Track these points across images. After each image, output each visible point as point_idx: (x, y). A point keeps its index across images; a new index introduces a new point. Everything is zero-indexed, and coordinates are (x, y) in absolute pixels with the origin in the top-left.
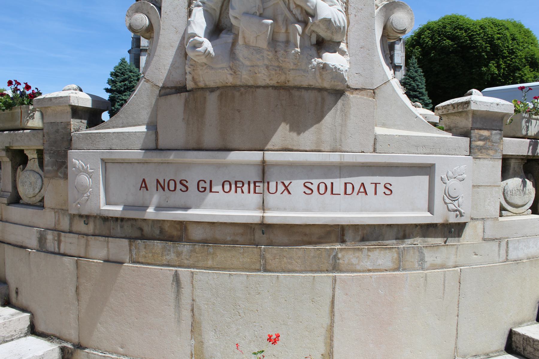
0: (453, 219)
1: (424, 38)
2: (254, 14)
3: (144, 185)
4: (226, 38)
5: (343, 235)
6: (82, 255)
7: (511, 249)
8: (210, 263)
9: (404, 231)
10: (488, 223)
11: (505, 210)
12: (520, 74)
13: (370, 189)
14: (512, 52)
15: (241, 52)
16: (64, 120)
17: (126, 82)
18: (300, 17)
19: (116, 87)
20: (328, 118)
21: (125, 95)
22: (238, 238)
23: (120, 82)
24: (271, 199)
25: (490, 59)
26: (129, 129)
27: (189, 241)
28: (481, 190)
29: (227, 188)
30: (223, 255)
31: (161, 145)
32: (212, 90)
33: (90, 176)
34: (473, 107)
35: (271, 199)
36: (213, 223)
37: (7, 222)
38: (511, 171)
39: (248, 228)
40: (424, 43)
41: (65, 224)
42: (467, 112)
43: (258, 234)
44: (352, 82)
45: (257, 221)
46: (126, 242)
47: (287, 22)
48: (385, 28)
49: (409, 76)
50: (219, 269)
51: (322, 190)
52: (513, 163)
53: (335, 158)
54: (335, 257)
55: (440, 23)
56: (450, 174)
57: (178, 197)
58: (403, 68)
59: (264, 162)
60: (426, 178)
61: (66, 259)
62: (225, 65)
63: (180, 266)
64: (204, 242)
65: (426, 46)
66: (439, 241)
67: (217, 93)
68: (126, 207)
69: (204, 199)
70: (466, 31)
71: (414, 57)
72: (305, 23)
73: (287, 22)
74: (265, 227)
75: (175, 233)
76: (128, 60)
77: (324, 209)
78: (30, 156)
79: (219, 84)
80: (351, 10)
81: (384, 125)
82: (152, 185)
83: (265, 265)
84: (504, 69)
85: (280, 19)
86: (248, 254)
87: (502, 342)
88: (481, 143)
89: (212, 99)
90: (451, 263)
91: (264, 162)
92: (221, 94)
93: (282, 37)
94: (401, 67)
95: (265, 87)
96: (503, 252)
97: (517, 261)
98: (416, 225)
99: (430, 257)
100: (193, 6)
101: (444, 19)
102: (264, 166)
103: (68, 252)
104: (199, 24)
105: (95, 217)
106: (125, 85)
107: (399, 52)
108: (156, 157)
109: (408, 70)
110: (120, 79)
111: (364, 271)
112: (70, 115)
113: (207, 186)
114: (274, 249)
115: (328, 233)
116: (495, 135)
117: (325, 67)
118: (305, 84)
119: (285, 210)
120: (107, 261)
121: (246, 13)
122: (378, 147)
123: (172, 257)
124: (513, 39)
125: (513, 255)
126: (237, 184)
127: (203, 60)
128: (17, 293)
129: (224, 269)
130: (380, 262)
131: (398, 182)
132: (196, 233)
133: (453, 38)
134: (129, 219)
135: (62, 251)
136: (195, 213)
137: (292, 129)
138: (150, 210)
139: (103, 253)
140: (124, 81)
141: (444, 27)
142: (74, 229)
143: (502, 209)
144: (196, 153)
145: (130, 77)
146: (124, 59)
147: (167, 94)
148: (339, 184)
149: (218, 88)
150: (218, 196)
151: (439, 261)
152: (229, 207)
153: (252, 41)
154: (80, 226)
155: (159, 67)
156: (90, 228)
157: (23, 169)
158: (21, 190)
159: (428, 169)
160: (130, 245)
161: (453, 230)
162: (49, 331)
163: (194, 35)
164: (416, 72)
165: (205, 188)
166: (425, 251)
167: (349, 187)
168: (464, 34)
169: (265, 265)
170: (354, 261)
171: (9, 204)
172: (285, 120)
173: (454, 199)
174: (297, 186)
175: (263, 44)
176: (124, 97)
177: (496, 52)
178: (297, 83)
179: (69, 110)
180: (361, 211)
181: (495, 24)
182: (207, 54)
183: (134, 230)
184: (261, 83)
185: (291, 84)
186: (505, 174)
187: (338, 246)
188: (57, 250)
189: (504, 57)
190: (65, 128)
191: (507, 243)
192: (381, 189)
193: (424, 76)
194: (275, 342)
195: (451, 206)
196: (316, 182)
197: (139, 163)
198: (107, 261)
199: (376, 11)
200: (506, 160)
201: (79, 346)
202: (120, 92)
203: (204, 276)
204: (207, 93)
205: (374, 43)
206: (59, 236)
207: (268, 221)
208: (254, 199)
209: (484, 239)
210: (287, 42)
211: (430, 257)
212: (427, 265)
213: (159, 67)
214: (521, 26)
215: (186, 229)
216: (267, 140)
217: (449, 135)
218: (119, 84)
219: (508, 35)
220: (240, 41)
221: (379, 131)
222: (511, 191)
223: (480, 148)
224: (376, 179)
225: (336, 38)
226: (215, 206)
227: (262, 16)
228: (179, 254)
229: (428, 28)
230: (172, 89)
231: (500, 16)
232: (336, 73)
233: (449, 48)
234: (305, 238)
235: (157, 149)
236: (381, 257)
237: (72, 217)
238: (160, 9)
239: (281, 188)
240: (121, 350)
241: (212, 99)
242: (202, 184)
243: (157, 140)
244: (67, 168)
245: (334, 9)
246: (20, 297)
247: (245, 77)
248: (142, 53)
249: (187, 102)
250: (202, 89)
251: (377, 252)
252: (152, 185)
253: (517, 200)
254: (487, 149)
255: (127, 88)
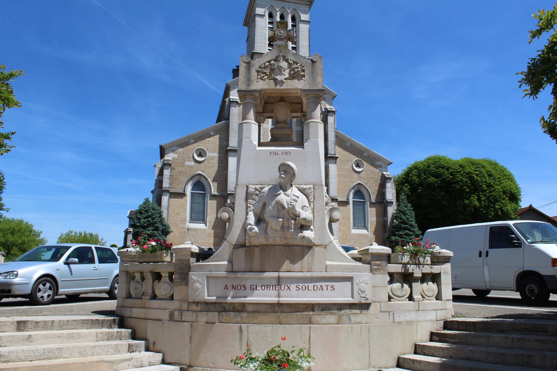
0: (363, 301)
1: (412, 176)
2: (275, 217)
3: (226, 287)
4: (263, 225)
5: (313, 308)
6: (194, 321)
7: (395, 317)
8: (256, 321)
9: (341, 307)
10: (382, 304)
11: (393, 298)
12: (499, 205)
13: (325, 288)
14: (489, 186)
15: (269, 231)
16: (187, 258)
17: (149, 219)
18: (293, 217)
19: (140, 223)
20: (306, 258)
21: (148, 230)
22: (268, 310)
23: (144, 219)
24: (282, 293)
25: (472, 193)
26: (219, 263)
27: (246, 312)
28: (377, 288)
29: (263, 288)
30: (261, 317)
31: (234, 269)
32: (257, 246)
33: (200, 283)
34: (370, 251)
35: (282, 293)
36: (257, 304)
37: (148, 308)
38: (395, 280)
39: (272, 305)
40: (412, 181)
41: (185, 306)
42: (369, 253)
43: (277, 308)
44: (316, 243)
45: (276, 302)
46: (217, 314)
47: (288, 220)
48: (330, 218)
49: (400, 211)
50: (260, 324)
51: (304, 288)
52: (395, 276)
53: (309, 274)
54: (310, 318)
55: (425, 163)
56: (361, 281)
57: (242, 292)
58: (394, 203)
59: (279, 277)
60: (350, 283)
61: (185, 323)
62: (263, 236)
63: (242, 323)
64: (253, 312)
65: (414, 183)
66: (358, 311)
67: (259, 248)
68: (217, 298)
69: (252, 293)
70: (447, 170)
71: (403, 194)
72: (295, 220)
73: (288, 220)
74: (279, 305)
75: (240, 308)
76: (151, 199)
77: (305, 297)
78: (163, 275)
79: (260, 244)
80: (315, 212)
81: (330, 260)
82: (230, 287)
83: (280, 321)
84: (484, 201)
85: (285, 218)
86: (272, 317)
87: (395, 363)
88: (376, 267)
89: (257, 250)
90: (364, 321)
91: (279, 277)
92: (261, 249)
93: (286, 225)
94: (392, 203)
95: (279, 245)
96: (391, 317)
97: (400, 323)
98: (346, 304)
99: (354, 319)
100: (248, 210)
101: (428, 159)
102: (279, 279)
103: (186, 320)
104: (252, 219)
105: (201, 303)
106: (148, 221)
107: (391, 190)
108: (232, 275)
109: (399, 206)
110: (145, 216)
111: (323, 324)
112: (190, 256)
113: (255, 287)
114: (284, 315)
115: (307, 307)
116: (383, 263)
117: (304, 237)
118: (296, 244)
119: (288, 297)
120: (207, 323)
121: (272, 216)
122: (328, 269)
123: (239, 319)
124: (490, 175)
125: (397, 320)
126: (268, 286)
127: (254, 235)
128: (154, 344)
129: (262, 324)
130: (330, 320)
131: (336, 285)
132: (250, 308)
133: (437, 175)
134: (219, 303)
135: (183, 320)
136: (249, 299)
137: (291, 263)
138: (229, 298)
139: (205, 319)
140: (147, 217)
141: (429, 167)
142: (190, 309)
143: (390, 298)
144: (250, 273)
145: (153, 214)
146: (148, 199)
147: (237, 248)
148: (311, 286)
149: (259, 246)
150: (259, 291)
151: (358, 320)
152: (264, 296)
153: (274, 227)
154: (194, 307)
155: (234, 235)
156: (199, 308)
157: (159, 282)
158: (157, 292)
159: (350, 279)
160: (219, 315)
161: (365, 306)
162: (173, 361)
163: (251, 225)
164: (406, 207)
165: (253, 288)
166: (351, 316)
167: (315, 287)
168: (446, 172)
169: (280, 321)
170: (319, 319)
171: (150, 299)
172: (288, 259)
173: (363, 292)
174: (293, 287)
175: (278, 228)
176: (147, 232)
177: (475, 187)
178: (293, 244)
179: (190, 254)
180: (321, 297)
181: (472, 162)
182: (256, 233)
183: (221, 308)
184: (278, 243)
185: (290, 244)
186: (391, 282)
187: (311, 313)
188: (180, 320)
189: (483, 191)
190: (187, 262)
191: (393, 314)
192: (329, 288)
193: (413, 210)
194: (284, 339)
195: (362, 295)
196: (301, 285)
197: (224, 277)
198: (207, 323)
199: (326, 211)
200: (391, 275)
201: (190, 366)
202: (144, 227)
203: (254, 328)
204: (255, 248)
205: (325, 226)
206: (182, 313)
207: (281, 302)
208: (275, 293)
209: (381, 312)
210: (288, 227)
211: (354, 319)
212: (352, 322)
213: (234, 235)
214: (496, 164)
215: (245, 306)
216: (280, 267)
217: (360, 264)
218: (143, 220)
219: (484, 171)
220: (269, 227)
221: (328, 263)
222: (395, 289)
223: (376, 270)
224: (327, 283)
225: (309, 224)
226: (258, 296)
227: (278, 218)
228: (242, 318)
229: (415, 167)
230: (239, 246)
231: (477, 156)
232: (309, 240)
233: (435, 185)
234: (297, 310)
235: (232, 271)
236: (331, 318)
237: (189, 303)
238: (234, 210)
239: (286, 288)
240: (212, 366)
241: (257, 250)
242: (252, 287)
243: (232, 267)
244: (188, 280)
245: (307, 213)
246: (156, 346)
247: (271, 241)
248: (164, 193)
249: (246, 251)
250: (253, 246)
251: (328, 316)
252: (230, 287)
253: (399, 294)
254: (379, 270)
255: (150, 224)
